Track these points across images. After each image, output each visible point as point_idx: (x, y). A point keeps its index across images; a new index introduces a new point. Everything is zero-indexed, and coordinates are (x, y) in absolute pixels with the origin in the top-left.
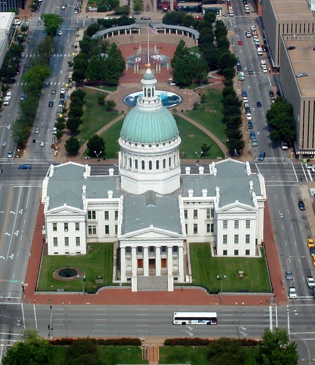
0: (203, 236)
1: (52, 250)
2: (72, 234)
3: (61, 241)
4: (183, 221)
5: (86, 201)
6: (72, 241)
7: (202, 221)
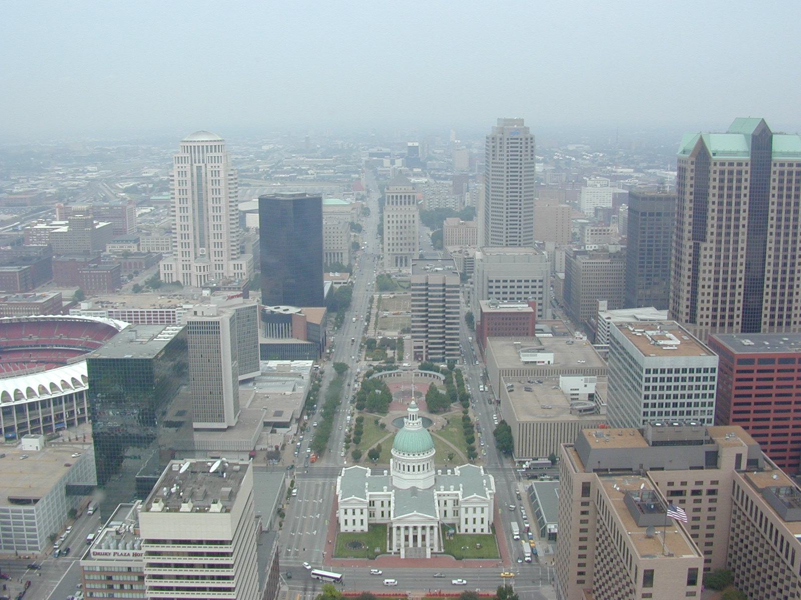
0: (450, 519)
1: (343, 528)
2: (358, 517)
3: (350, 522)
4: (437, 508)
5: (368, 494)
6: (358, 522)
7: (450, 507)
